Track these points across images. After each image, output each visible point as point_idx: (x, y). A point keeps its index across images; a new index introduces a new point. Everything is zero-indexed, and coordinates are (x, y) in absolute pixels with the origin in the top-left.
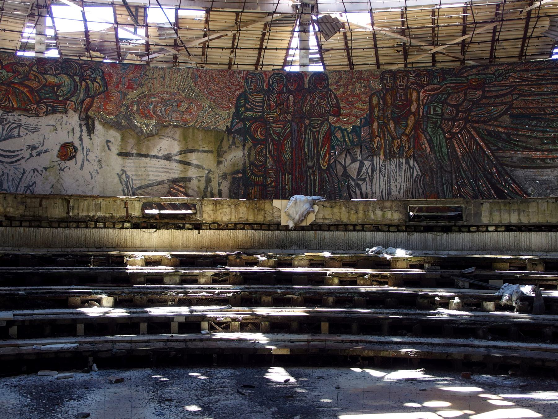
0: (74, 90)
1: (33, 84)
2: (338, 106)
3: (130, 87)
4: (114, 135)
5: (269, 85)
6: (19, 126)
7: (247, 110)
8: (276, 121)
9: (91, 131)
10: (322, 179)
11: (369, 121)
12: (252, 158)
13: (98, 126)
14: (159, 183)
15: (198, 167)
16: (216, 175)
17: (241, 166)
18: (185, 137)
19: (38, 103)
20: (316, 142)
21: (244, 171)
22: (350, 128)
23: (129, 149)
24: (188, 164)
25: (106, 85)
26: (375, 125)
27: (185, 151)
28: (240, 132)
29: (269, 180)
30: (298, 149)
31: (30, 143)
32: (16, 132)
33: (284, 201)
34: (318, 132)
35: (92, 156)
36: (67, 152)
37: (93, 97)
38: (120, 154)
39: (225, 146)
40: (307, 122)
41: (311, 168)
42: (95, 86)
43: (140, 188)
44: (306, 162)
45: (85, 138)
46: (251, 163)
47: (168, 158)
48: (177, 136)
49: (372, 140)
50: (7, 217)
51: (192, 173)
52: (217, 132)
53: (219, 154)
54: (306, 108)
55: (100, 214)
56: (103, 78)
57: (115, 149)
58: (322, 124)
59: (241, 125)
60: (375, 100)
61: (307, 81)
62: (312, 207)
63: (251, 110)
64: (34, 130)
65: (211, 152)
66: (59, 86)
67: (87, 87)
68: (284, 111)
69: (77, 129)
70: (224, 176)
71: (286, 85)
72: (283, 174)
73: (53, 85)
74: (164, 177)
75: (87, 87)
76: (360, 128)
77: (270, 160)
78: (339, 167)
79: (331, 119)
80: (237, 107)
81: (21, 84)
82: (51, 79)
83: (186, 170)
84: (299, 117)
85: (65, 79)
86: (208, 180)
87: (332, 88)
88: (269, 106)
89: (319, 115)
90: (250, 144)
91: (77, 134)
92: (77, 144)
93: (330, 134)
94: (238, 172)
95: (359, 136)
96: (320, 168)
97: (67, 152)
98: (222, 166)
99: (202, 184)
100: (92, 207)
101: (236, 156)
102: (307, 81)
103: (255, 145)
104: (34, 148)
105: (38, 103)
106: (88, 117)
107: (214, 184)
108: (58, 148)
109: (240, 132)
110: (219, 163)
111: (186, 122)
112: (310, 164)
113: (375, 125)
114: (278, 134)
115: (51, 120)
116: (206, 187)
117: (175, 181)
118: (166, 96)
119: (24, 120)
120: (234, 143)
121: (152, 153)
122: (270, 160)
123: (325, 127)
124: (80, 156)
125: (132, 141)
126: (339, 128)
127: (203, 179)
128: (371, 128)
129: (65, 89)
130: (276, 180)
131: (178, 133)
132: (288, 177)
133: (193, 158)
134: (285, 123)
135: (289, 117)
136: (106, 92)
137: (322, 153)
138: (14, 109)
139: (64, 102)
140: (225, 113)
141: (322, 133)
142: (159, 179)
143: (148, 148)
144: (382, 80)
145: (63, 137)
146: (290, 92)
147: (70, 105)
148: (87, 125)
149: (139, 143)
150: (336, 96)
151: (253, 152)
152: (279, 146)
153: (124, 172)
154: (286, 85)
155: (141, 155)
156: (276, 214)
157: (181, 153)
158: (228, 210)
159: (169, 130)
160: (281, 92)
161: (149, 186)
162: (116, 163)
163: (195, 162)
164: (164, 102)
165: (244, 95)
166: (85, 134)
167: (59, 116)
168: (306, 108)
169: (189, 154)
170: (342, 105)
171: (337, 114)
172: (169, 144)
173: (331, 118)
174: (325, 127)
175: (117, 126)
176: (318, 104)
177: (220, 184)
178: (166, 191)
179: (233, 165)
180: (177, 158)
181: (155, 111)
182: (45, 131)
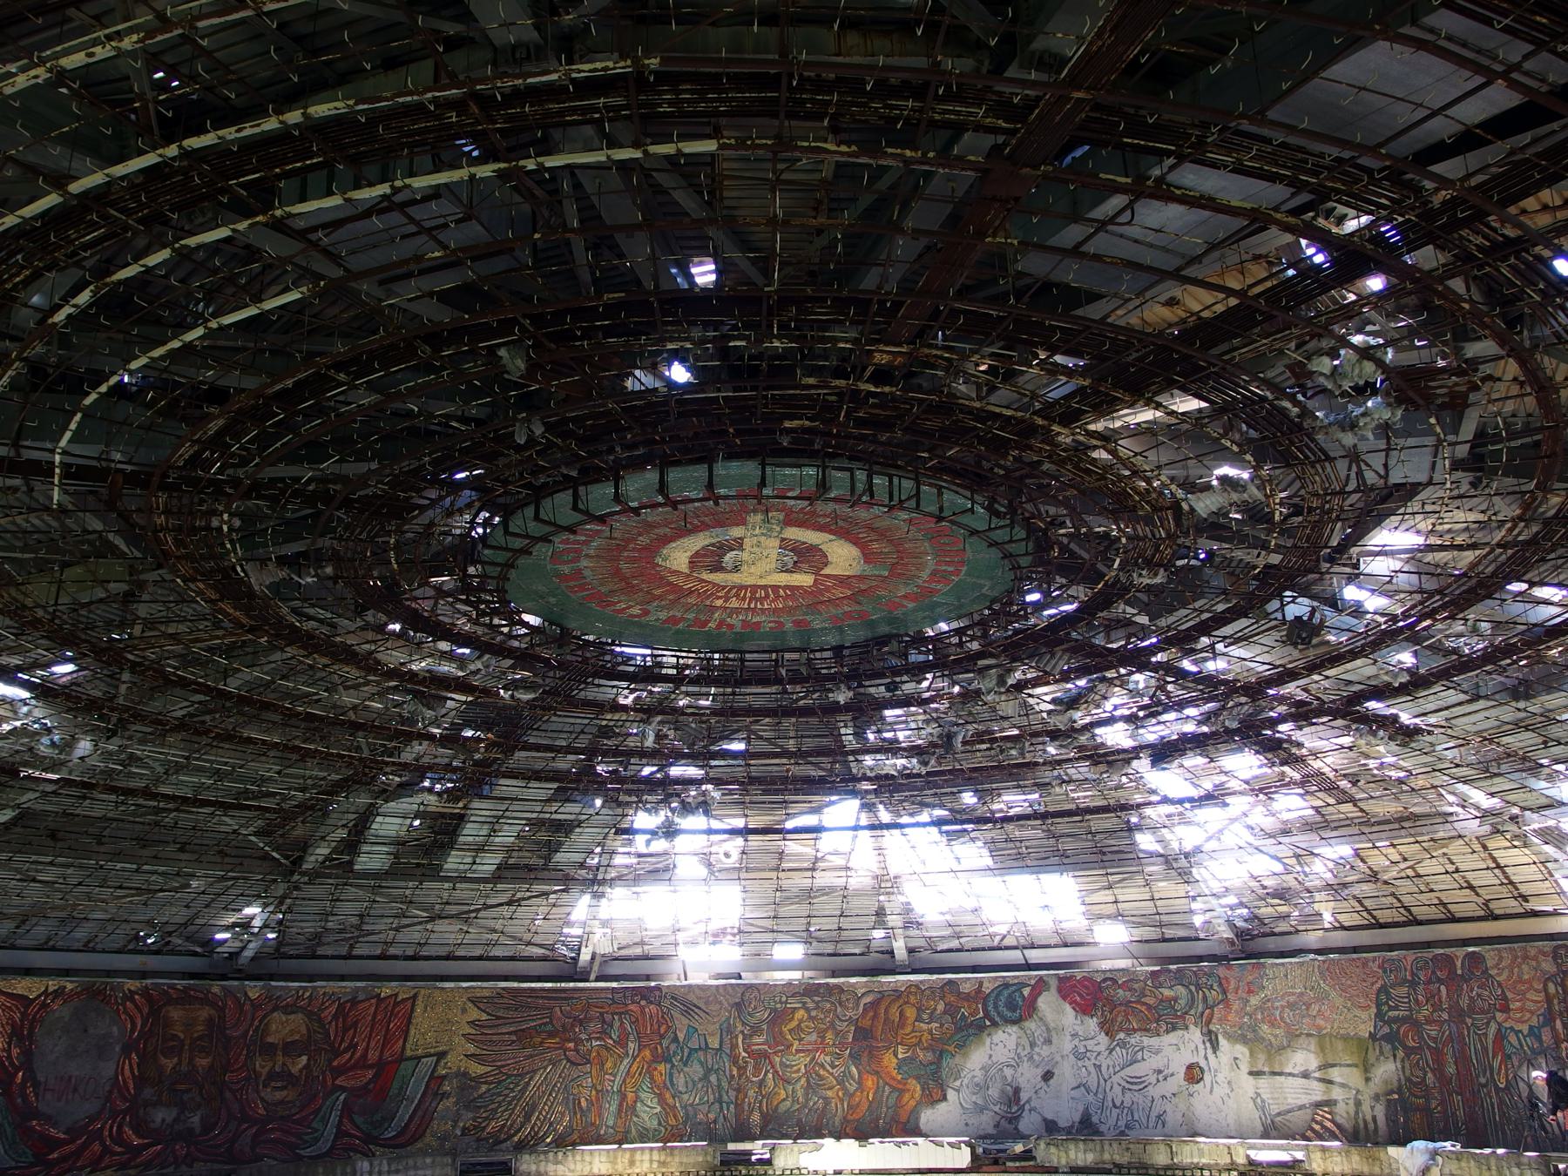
0: (1192, 1002)
1: (1150, 1001)
2: (1505, 998)
3: (1250, 992)
4: (1241, 1050)
5: (1413, 974)
6: (1142, 1049)
7: (1391, 1008)
8: (1429, 1021)
9: (1215, 1048)
10: (1501, 1102)
11: (1549, 1019)
12: (1408, 1072)
13: (1222, 1041)
14: (1301, 1108)
15: (1343, 1085)
16: (1366, 1097)
17: (1396, 1084)
18: (1322, 1048)
19: (1157, 1021)
20: (1485, 1049)
21: (1399, 1091)
22: (1525, 1028)
23: (1260, 1067)
24: (1330, 1082)
25: (1224, 992)
26: (1558, 1023)
27: (1325, 1066)
28: (1388, 1038)
29: (1434, 1104)
30: (1462, 1059)
31: (1155, 1067)
32: (1139, 1055)
33: (1401, 1149)
34: (1485, 1034)
35: (1220, 1078)
36: (1194, 1074)
37: (1212, 1008)
38: (1251, 1073)
39: (1372, 1057)
40: (1469, 1021)
41: (1485, 1086)
42: (1213, 995)
43: (1279, 1114)
44: (1478, 1076)
45: (1211, 1056)
46: (1408, 1080)
47: (1305, 1075)
48: (1312, 1047)
49: (1558, 1047)
50: (1116, 1165)
51: (1337, 1094)
52: (1360, 1039)
53: (1366, 1068)
54: (1464, 1003)
55: (1204, 1161)
56: (1220, 984)
57: (1245, 1068)
58: (1488, 1023)
59: (1386, 1030)
60: (1551, 988)
61: (1459, 964)
62: (1433, 1159)
63: (1396, 1008)
64: (1157, 1053)
65: (1356, 1066)
66: (1176, 999)
67: (1205, 997)
68: (1437, 1007)
69: (1201, 1047)
70: (1376, 1097)
71: (1434, 972)
72: (1450, 1095)
73: (1169, 1000)
74: (1305, 1100)
75: (1205, 997)
76: (1539, 1028)
77: (1430, 1075)
78: (1521, 1084)
79: (1500, 1016)
80: (1378, 1006)
81: (1138, 1002)
82: (1167, 992)
83: (1328, 1091)
84: (1458, 1015)
85: (1181, 990)
86: (1358, 1104)
87: (1493, 972)
88: (1417, 1000)
89: (1483, 1012)
90: (1400, 1054)
91: (1202, 1053)
92: (1203, 1064)
93: (1500, 1037)
94: (1391, 1092)
95: (1540, 1041)
96: (1496, 1086)
97: (1194, 1074)
98: (1371, 1084)
99: (1352, 1109)
100: (1196, 1153)
101: (1387, 1070)
102: (1459, 964)
103: (1408, 1055)
104: (1160, 1072)
105: (1157, 1021)
106: (1210, 1032)
107: (1366, 1108)
108: (1183, 1070)
109: (1388, 1038)
110: (1368, 1080)
111: (1320, 1029)
112: (1483, 1080)
113: (1558, 1023)
114: (1434, 1040)
115: (1172, 1038)
116: (1357, 1113)
117: (1318, 1105)
118: (1292, 999)
119: (1146, 1041)
120: (1382, 1053)
121: (1287, 1070)
122: (1430, 1075)
123: (1493, 1027)
124: (1207, 1077)
125: (1262, 1057)
126: (1512, 1028)
127: (1351, 1102)
128: (1553, 1029)
129: (1182, 1002)
130: (1442, 1103)
131: (1313, 1044)
132: (1457, 1098)
133: (1335, 1074)
134: (1441, 1023)
135: (1445, 1016)
136: (1225, 1001)
137: (1496, 1064)
138: (1135, 1031)
139: (1182, 1017)
140: (1364, 1015)
141: (1491, 1037)
142: (1300, 1103)
143: (1281, 1064)
144: (1555, 958)
145: (1188, 1057)
146: (1440, 981)
147: (1190, 1019)
148: (1210, 1040)
149: (1270, 1058)
150: (1500, 985)
151: (1407, 1065)
152: (1438, 1054)
153: (1258, 1095)
154: (1434, 972)
155: (1274, 1073)
156: (1394, 1166)
157: (1320, 1069)
158: (1338, 1159)
159: (1302, 1040)
160: (1429, 982)
161: (1289, 1111)
162: (1248, 1085)
163: (1338, 1080)
164: (1291, 1006)
165: (1383, 990)
166: (1210, 1051)
167: (1180, 1033)
168: (1464, 1003)
169: (1330, 1070)
170: (1510, 995)
171: (1505, 1009)
172: (1303, 1058)
173: (1498, 1015)
174: (1493, 1027)
175: (1244, 1040)
176: (1479, 995)
177: (1372, 1108)
178: (1309, 1117)
179: (1386, 1082)
180: (1317, 1075)
181: (1282, 1018)
182: (1168, 1051)
